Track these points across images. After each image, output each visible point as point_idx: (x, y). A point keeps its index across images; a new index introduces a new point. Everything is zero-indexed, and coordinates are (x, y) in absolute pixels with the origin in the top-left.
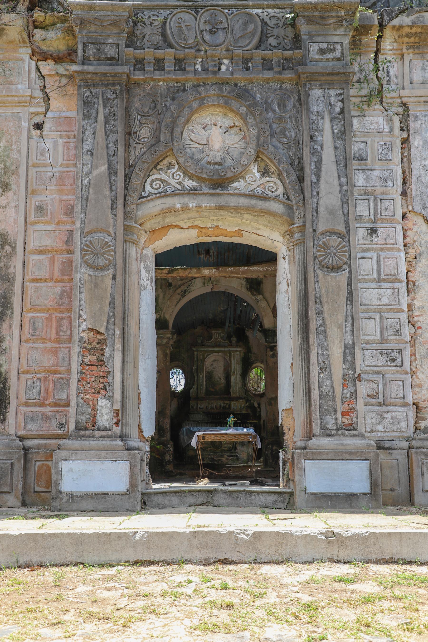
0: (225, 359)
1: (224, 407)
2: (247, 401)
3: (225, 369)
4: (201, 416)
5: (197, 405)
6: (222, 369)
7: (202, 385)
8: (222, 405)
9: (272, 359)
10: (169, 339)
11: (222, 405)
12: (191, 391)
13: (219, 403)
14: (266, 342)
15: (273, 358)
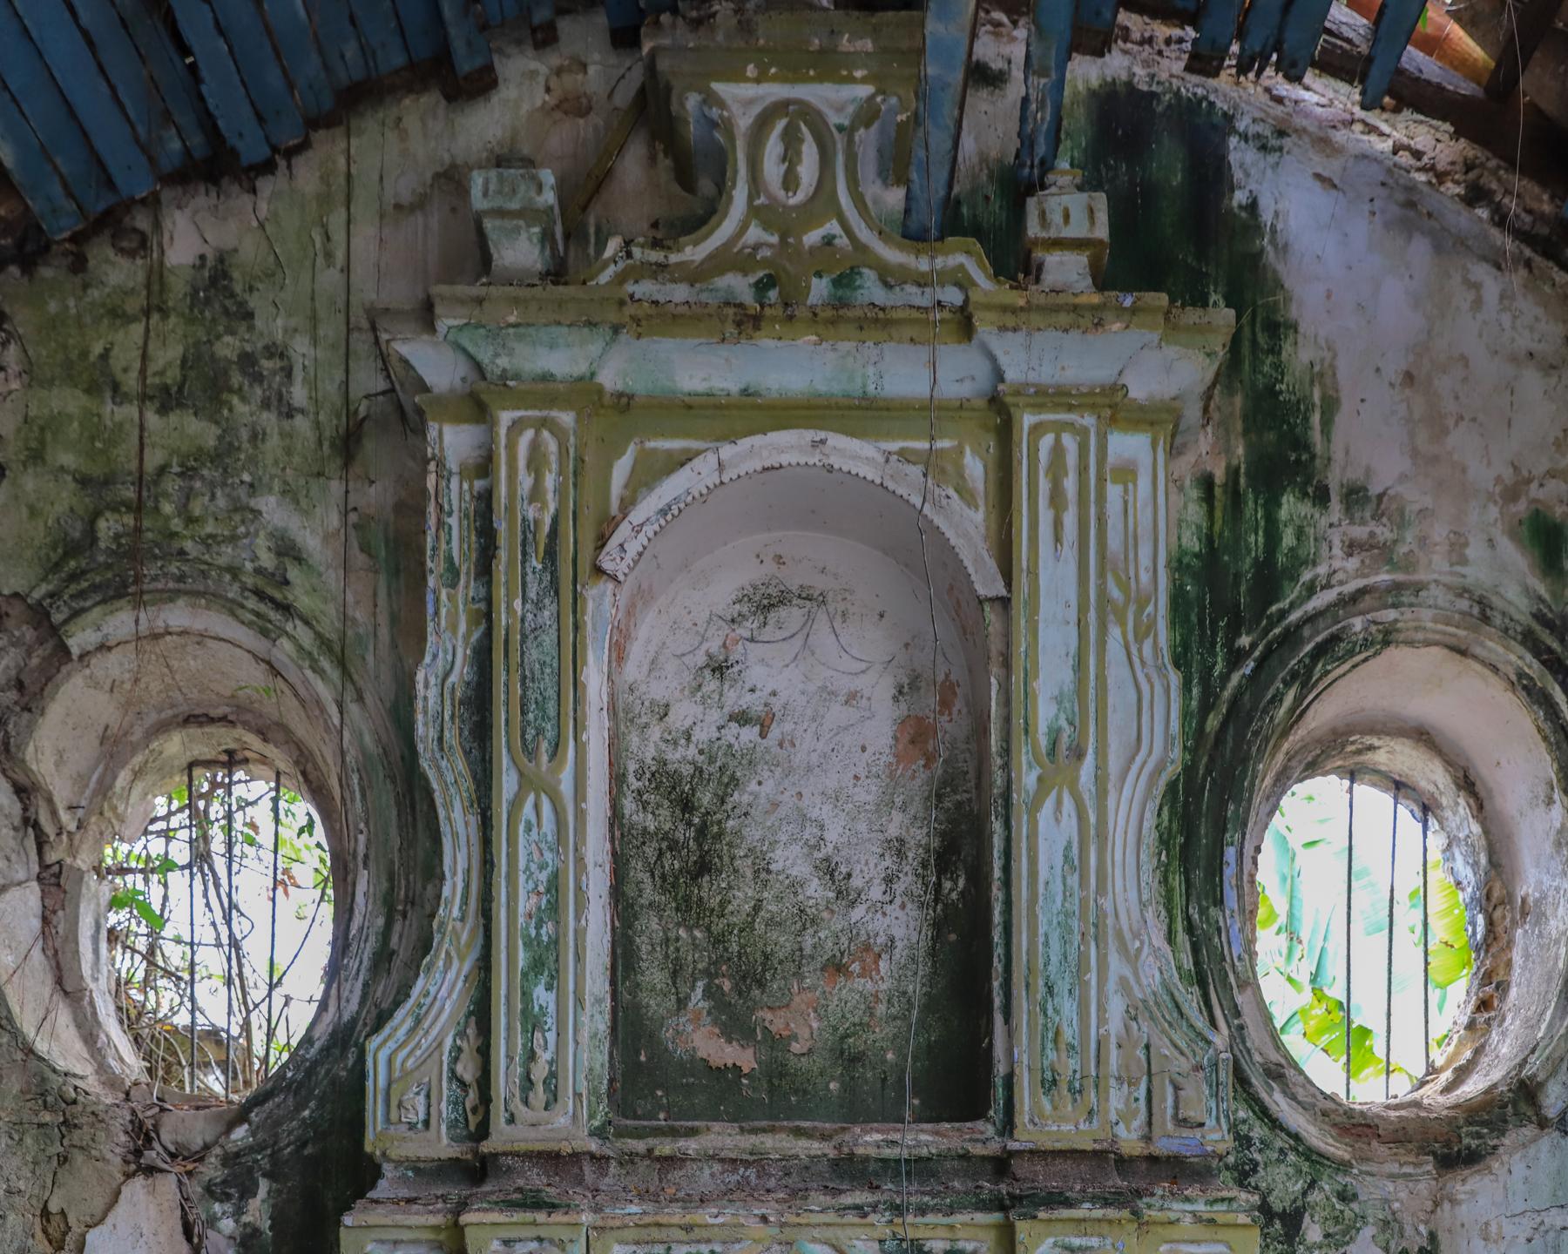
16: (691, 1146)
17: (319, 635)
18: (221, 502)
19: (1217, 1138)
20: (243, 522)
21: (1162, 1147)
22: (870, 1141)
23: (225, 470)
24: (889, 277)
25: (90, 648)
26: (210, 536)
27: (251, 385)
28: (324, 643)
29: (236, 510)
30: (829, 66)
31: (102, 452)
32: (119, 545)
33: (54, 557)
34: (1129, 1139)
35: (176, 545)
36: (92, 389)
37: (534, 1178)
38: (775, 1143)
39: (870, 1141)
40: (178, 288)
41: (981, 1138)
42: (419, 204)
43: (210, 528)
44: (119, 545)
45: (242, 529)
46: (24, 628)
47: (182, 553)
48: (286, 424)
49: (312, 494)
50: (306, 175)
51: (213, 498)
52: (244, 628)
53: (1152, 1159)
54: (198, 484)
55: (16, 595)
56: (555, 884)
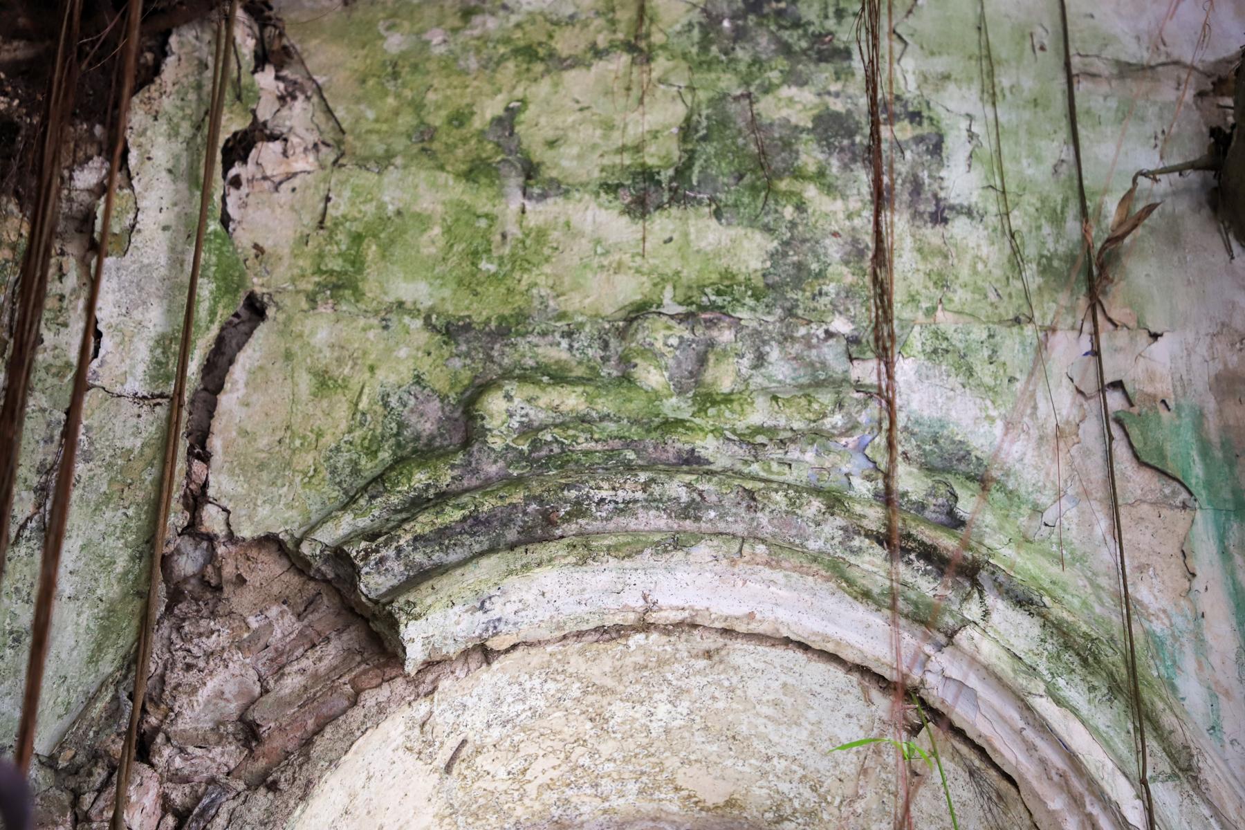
17: (1060, 631)
18: (780, 368)
20: (840, 405)
23: (790, 312)
25: (452, 650)
26: (759, 430)
27: (845, 167)
29: (818, 384)
31: (494, 278)
32: (536, 445)
33: (369, 467)
35: (679, 443)
43: (759, 413)
44: (536, 445)
45: (837, 419)
46: (274, 611)
47: (691, 461)
48: (932, 234)
49: (1004, 355)
51: (760, 360)
52: (861, 612)
54: (725, 336)
55: (269, 541)
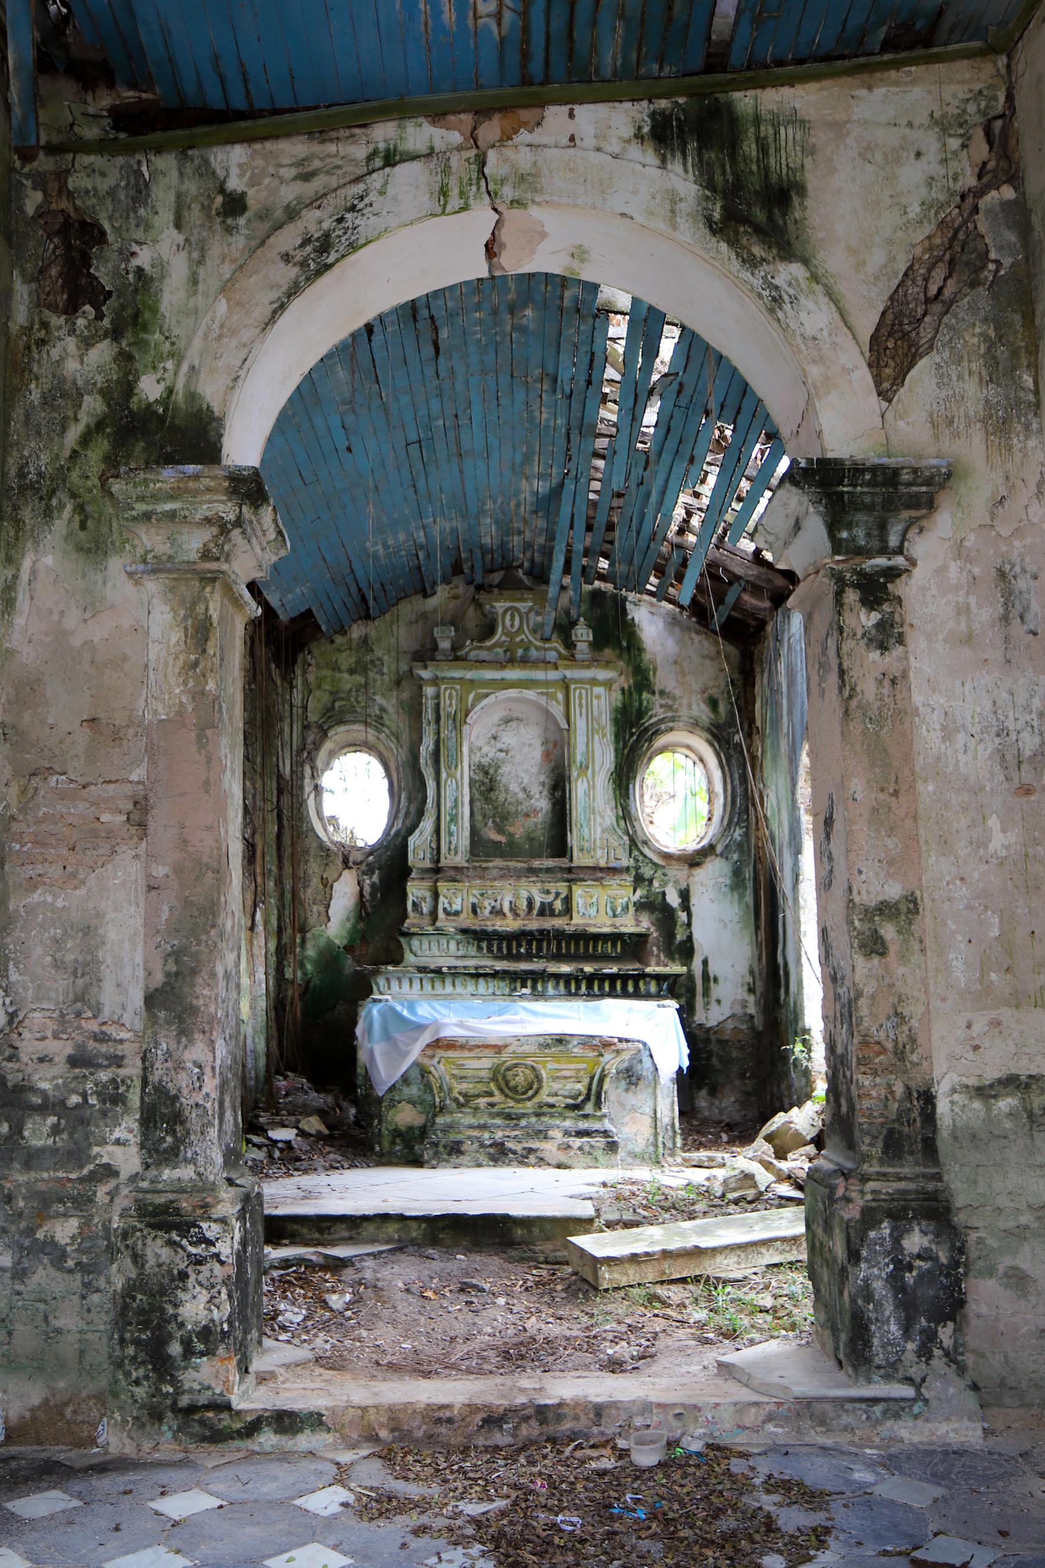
0: (548, 714)
1: (546, 910)
2: (639, 880)
3: (547, 755)
4: (453, 945)
5: (436, 896)
6: (537, 753)
7: (454, 819)
8: (538, 900)
9: (875, 655)
10: (224, 528)
11: (538, 900)
12: (412, 841)
13: (524, 894)
14: (837, 547)
15: (883, 647)
16: (491, 865)
19: (625, 862)
21: (611, 865)
22: (536, 863)
24: (537, 648)
28: (393, 734)
30: (522, 600)
34: (603, 863)
36: (333, 669)
37: (452, 873)
38: (512, 864)
39: (536, 863)
40: (354, 643)
41: (563, 862)
42: (416, 622)
50: (388, 616)
53: (609, 869)
56: (456, 800)
